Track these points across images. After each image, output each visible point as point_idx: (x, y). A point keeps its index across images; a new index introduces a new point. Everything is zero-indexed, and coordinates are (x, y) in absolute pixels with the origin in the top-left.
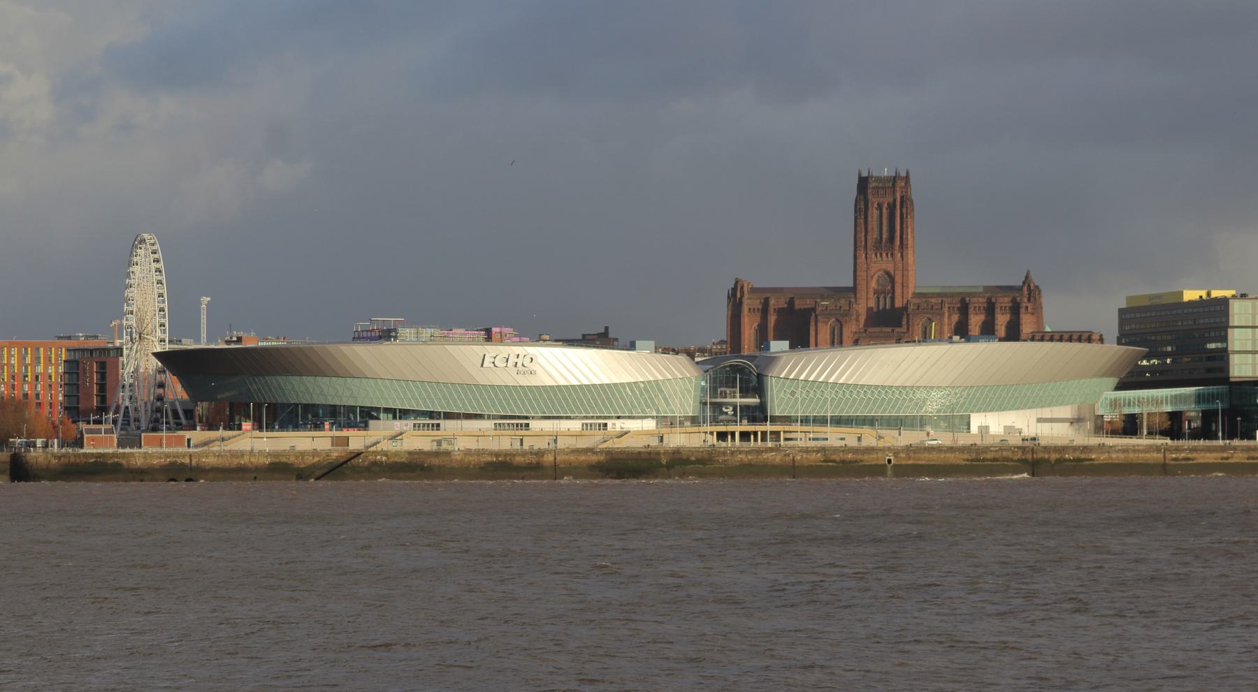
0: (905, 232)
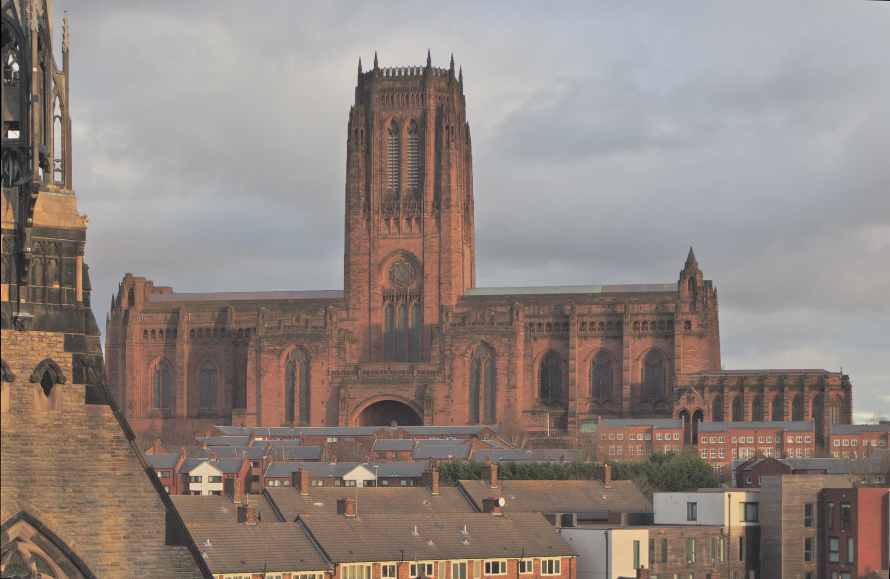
0: (445, 177)
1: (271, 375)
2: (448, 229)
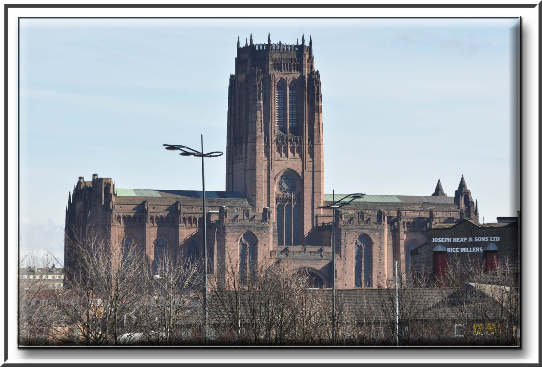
2: (319, 156)
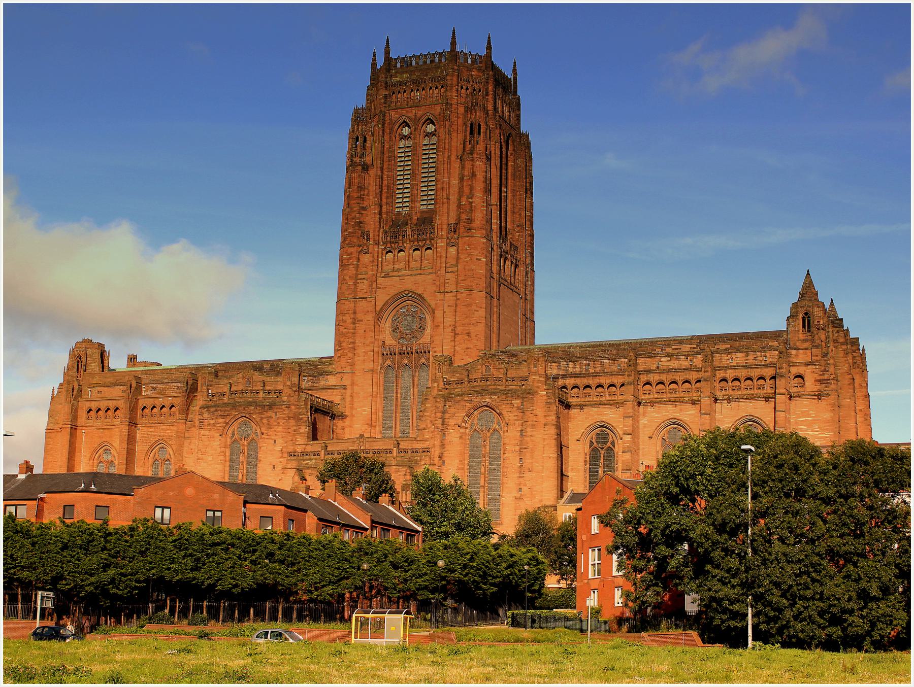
1: (210, 458)
